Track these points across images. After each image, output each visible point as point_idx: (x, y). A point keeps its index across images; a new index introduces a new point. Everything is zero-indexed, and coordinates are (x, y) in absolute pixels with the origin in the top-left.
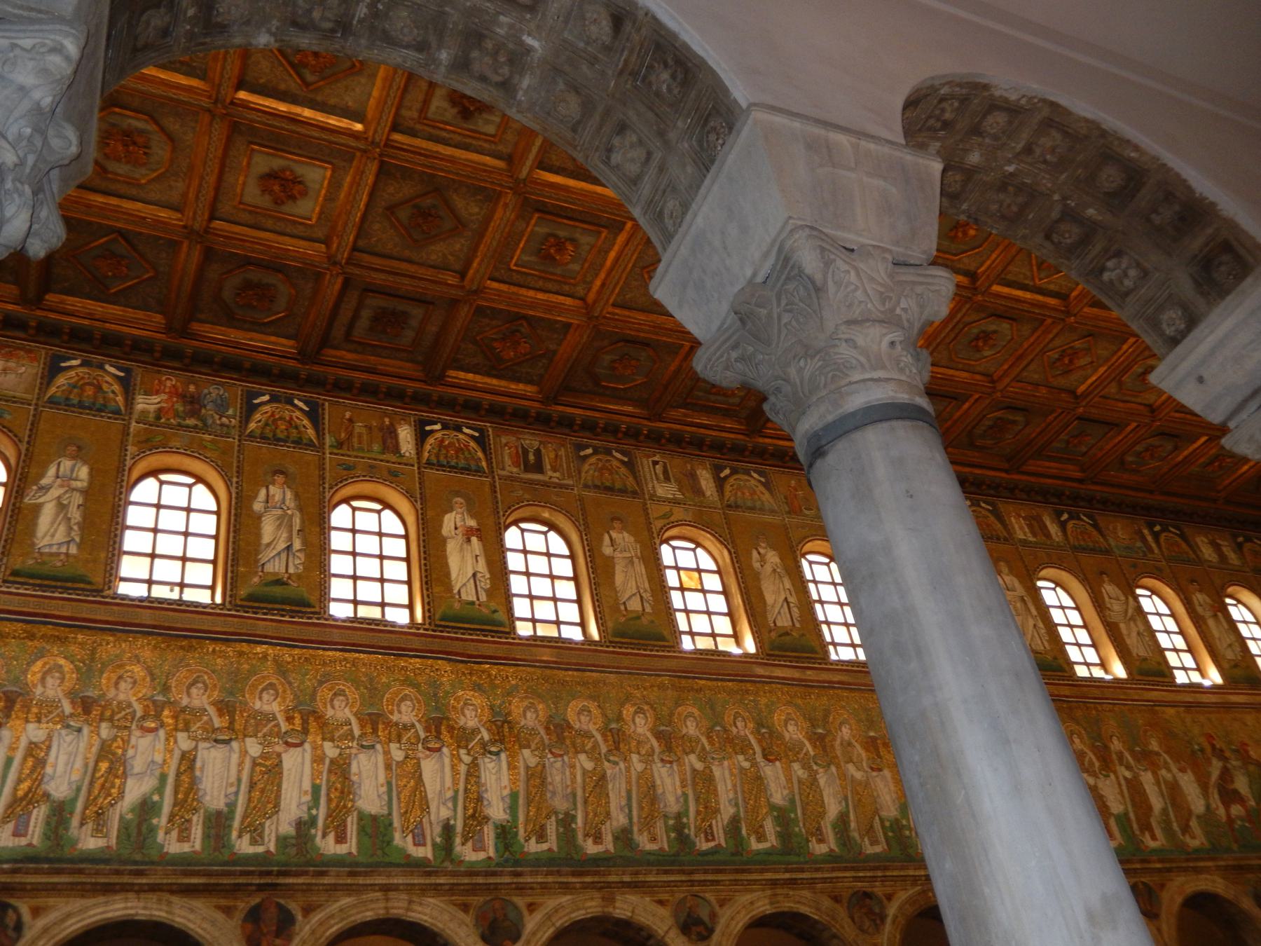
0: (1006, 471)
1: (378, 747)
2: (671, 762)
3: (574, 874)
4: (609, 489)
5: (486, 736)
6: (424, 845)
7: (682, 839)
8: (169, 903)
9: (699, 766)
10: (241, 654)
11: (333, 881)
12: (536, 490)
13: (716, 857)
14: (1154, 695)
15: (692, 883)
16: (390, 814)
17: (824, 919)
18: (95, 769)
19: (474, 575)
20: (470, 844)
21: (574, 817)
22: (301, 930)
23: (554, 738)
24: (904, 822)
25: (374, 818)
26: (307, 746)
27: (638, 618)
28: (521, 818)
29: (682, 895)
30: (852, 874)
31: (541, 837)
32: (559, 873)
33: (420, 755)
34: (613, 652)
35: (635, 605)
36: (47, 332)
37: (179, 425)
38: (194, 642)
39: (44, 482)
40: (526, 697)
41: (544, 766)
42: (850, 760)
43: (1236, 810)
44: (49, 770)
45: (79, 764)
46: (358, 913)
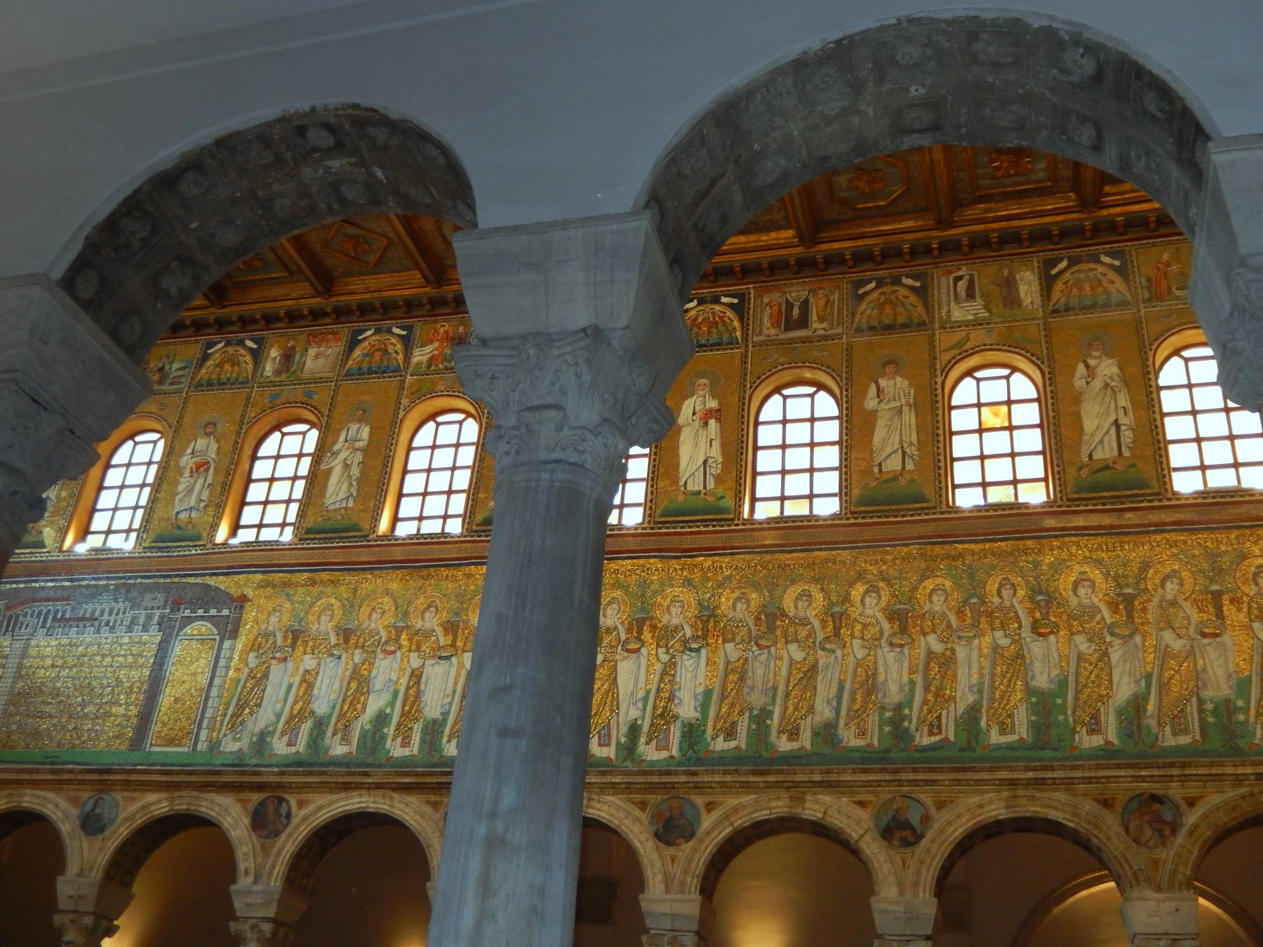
3: (754, 773)
4: (889, 328)
5: (689, 633)
6: (609, 745)
8: (391, 798)
10: (469, 576)
12: (794, 349)
13: (939, 754)
15: (900, 783)
18: (347, 689)
19: (705, 462)
20: (654, 743)
21: (771, 712)
23: (764, 628)
24: (1240, 703)
27: (895, 479)
28: (712, 715)
29: (889, 796)
30: (1132, 772)
31: (730, 734)
33: (618, 657)
34: (854, 525)
35: (894, 464)
36: (341, 314)
37: (446, 368)
38: (432, 570)
39: (336, 448)
40: (739, 588)
41: (746, 660)
44: (315, 692)
45: (336, 687)
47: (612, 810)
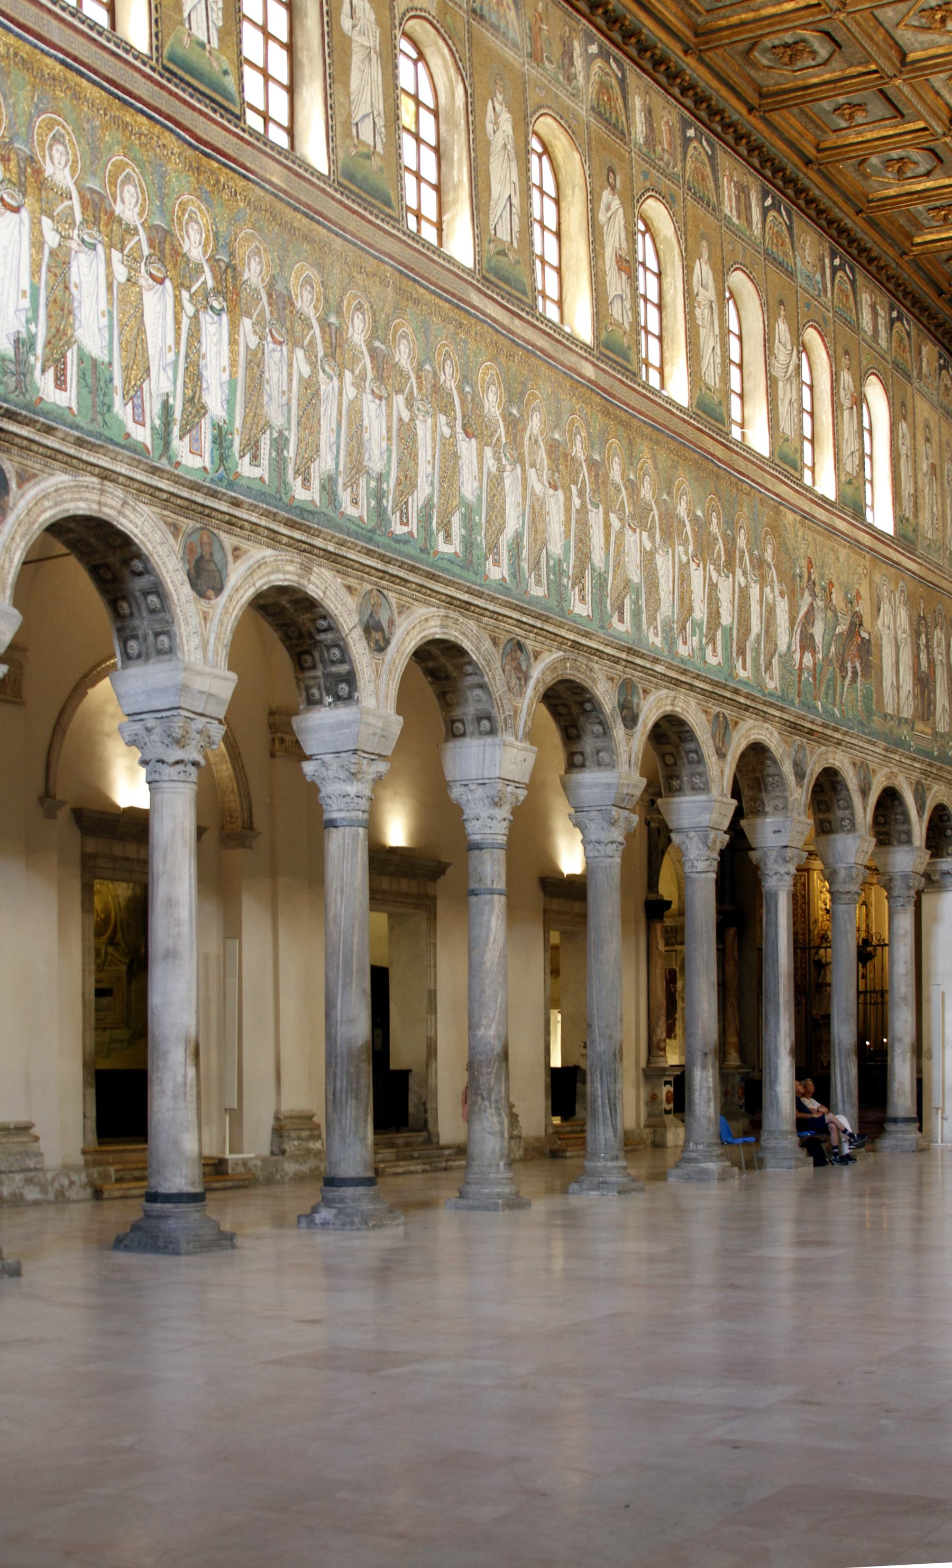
0: (751, 110)
1: (100, 248)
2: (380, 398)
5: (210, 284)
7: (380, 512)
9: (406, 416)
11: (56, 445)
14: (782, 490)
16: (110, 364)
17: (481, 663)
20: (187, 439)
21: (287, 440)
22: (15, 505)
25: (95, 363)
26: (24, 213)
27: (368, 157)
29: (369, 587)
32: (274, 517)
33: (142, 282)
42: (533, 465)
43: (808, 659)
46: (72, 500)
47: (147, 528)
